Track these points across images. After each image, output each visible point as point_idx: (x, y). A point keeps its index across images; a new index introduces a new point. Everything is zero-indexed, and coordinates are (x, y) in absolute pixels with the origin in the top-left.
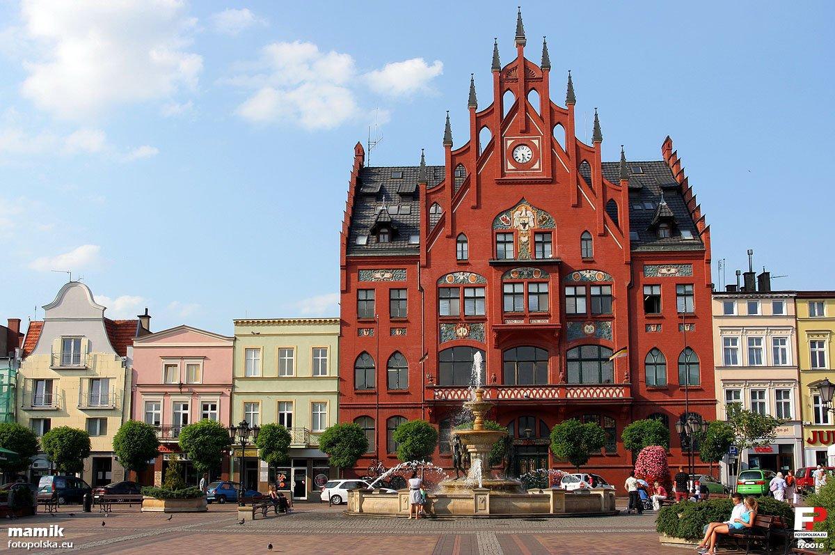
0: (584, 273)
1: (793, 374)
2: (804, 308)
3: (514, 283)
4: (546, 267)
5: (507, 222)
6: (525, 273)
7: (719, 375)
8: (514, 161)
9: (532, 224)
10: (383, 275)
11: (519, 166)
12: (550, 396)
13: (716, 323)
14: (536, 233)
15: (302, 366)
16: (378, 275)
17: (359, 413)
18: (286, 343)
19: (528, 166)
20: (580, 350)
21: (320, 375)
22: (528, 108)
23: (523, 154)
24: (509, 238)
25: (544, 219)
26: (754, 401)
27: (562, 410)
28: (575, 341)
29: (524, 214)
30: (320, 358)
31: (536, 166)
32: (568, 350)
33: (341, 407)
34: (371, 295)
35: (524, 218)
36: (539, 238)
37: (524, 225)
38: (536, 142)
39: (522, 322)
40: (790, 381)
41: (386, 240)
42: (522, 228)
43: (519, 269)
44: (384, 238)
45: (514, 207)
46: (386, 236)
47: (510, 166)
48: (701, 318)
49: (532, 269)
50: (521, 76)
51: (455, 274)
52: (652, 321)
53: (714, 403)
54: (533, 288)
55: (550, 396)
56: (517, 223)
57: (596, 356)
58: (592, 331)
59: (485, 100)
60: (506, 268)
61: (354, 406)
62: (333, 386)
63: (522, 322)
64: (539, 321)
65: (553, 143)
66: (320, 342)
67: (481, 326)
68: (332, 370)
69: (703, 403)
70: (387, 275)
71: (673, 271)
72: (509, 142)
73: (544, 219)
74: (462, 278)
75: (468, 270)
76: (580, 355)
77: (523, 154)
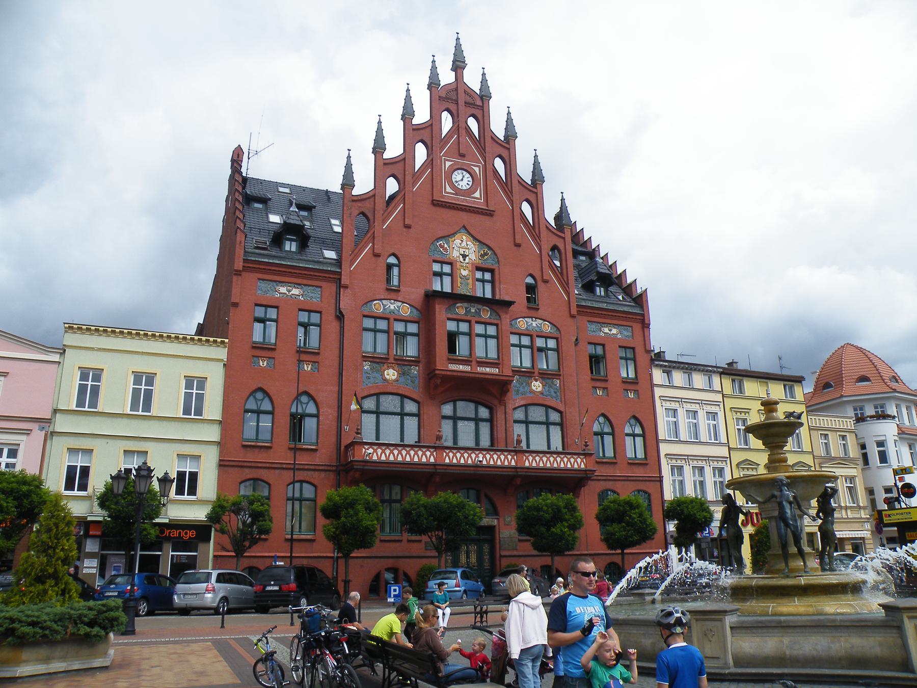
0: (529, 320)
1: (724, 451)
2: (727, 383)
3: (458, 320)
4: (495, 308)
5: (446, 250)
6: (473, 311)
7: (664, 449)
8: (452, 186)
9: (473, 257)
10: (289, 291)
11: (458, 191)
12: (506, 463)
13: (658, 392)
14: (478, 269)
15: (168, 398)
16: (283, 290)
17: (248, 473)
18: (145, 365)
19: (469, 192)
20: (526, 412)
21: (192, 417)
22: (468, 130)
23: (462, 180)
24: (447, 269)
25: (485, 254)
26: (681, 478)
27: (518, 481)
28: (523, 399)
29: (464, 244)
30: (195, 391)
31: (477, 195)
32: (515, 409)
33: (223, 465)
34: (272, 313)
35: (463, 249)
36: (479, 275)
37: (464, 256)
38: (477, 169)
39: (468, 368)
40: (723, 459)
41: (294, 249)
42: (462, 259)
43: (466, 305)
44: (291, 246)
45: (453, 234)
46: (294, 245)
47: (449, 189)
48: (640, 386)
49: (480, 307)
50: (461, 99)
51: (385, 302)
52: (598, 384)
53: (660, 479)
54: (479, 329)
55: (506, 463)
56: (456, 254)
57: (544, 419)
58: (540, 389)
59: (422, 116)
60: (451, 302)
61: (240, 464)
62: (213, 433)
63: (468, 368)
64: (488, 369)
65: (495, 172)
66: (197, 370)
67: (415, 371)
68: (213, 408)
69: (650, 480)
70: (295, 291)
71: (614, 331)
72: (448, 164)
73: (485, 254)
74: (392, 307)
75: (399, 299)
76: (526, 416)
77: (462, 180)
